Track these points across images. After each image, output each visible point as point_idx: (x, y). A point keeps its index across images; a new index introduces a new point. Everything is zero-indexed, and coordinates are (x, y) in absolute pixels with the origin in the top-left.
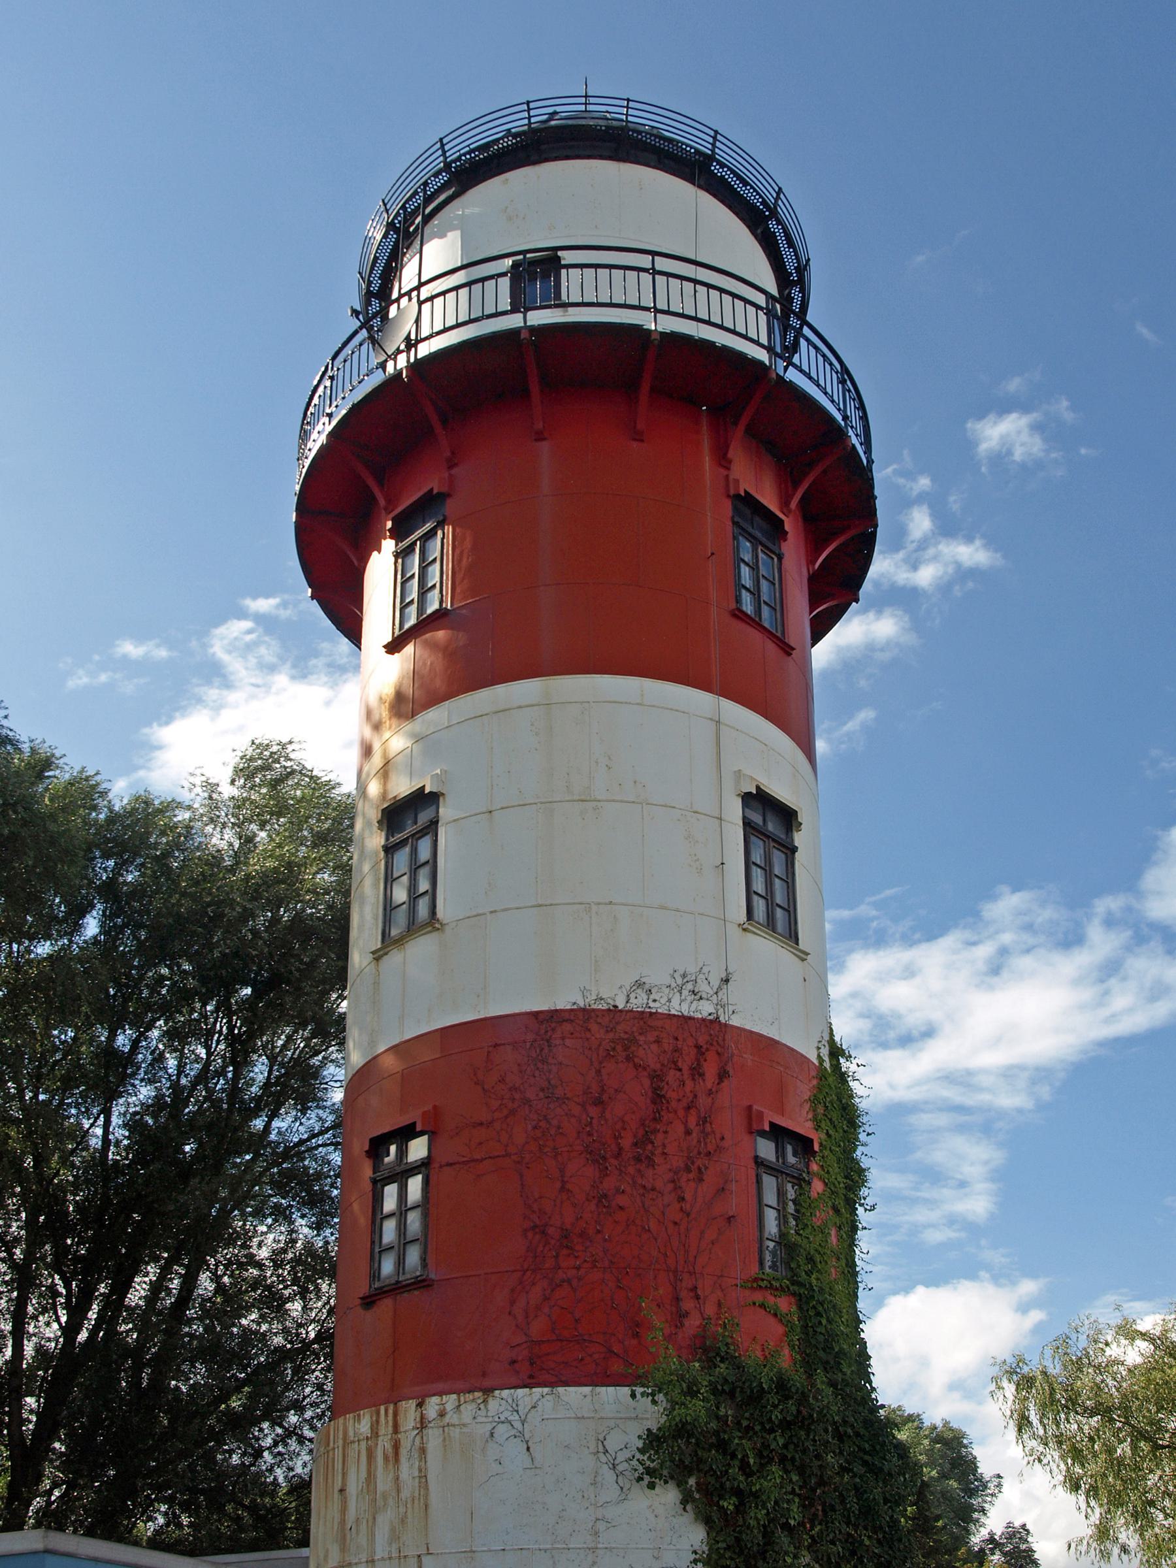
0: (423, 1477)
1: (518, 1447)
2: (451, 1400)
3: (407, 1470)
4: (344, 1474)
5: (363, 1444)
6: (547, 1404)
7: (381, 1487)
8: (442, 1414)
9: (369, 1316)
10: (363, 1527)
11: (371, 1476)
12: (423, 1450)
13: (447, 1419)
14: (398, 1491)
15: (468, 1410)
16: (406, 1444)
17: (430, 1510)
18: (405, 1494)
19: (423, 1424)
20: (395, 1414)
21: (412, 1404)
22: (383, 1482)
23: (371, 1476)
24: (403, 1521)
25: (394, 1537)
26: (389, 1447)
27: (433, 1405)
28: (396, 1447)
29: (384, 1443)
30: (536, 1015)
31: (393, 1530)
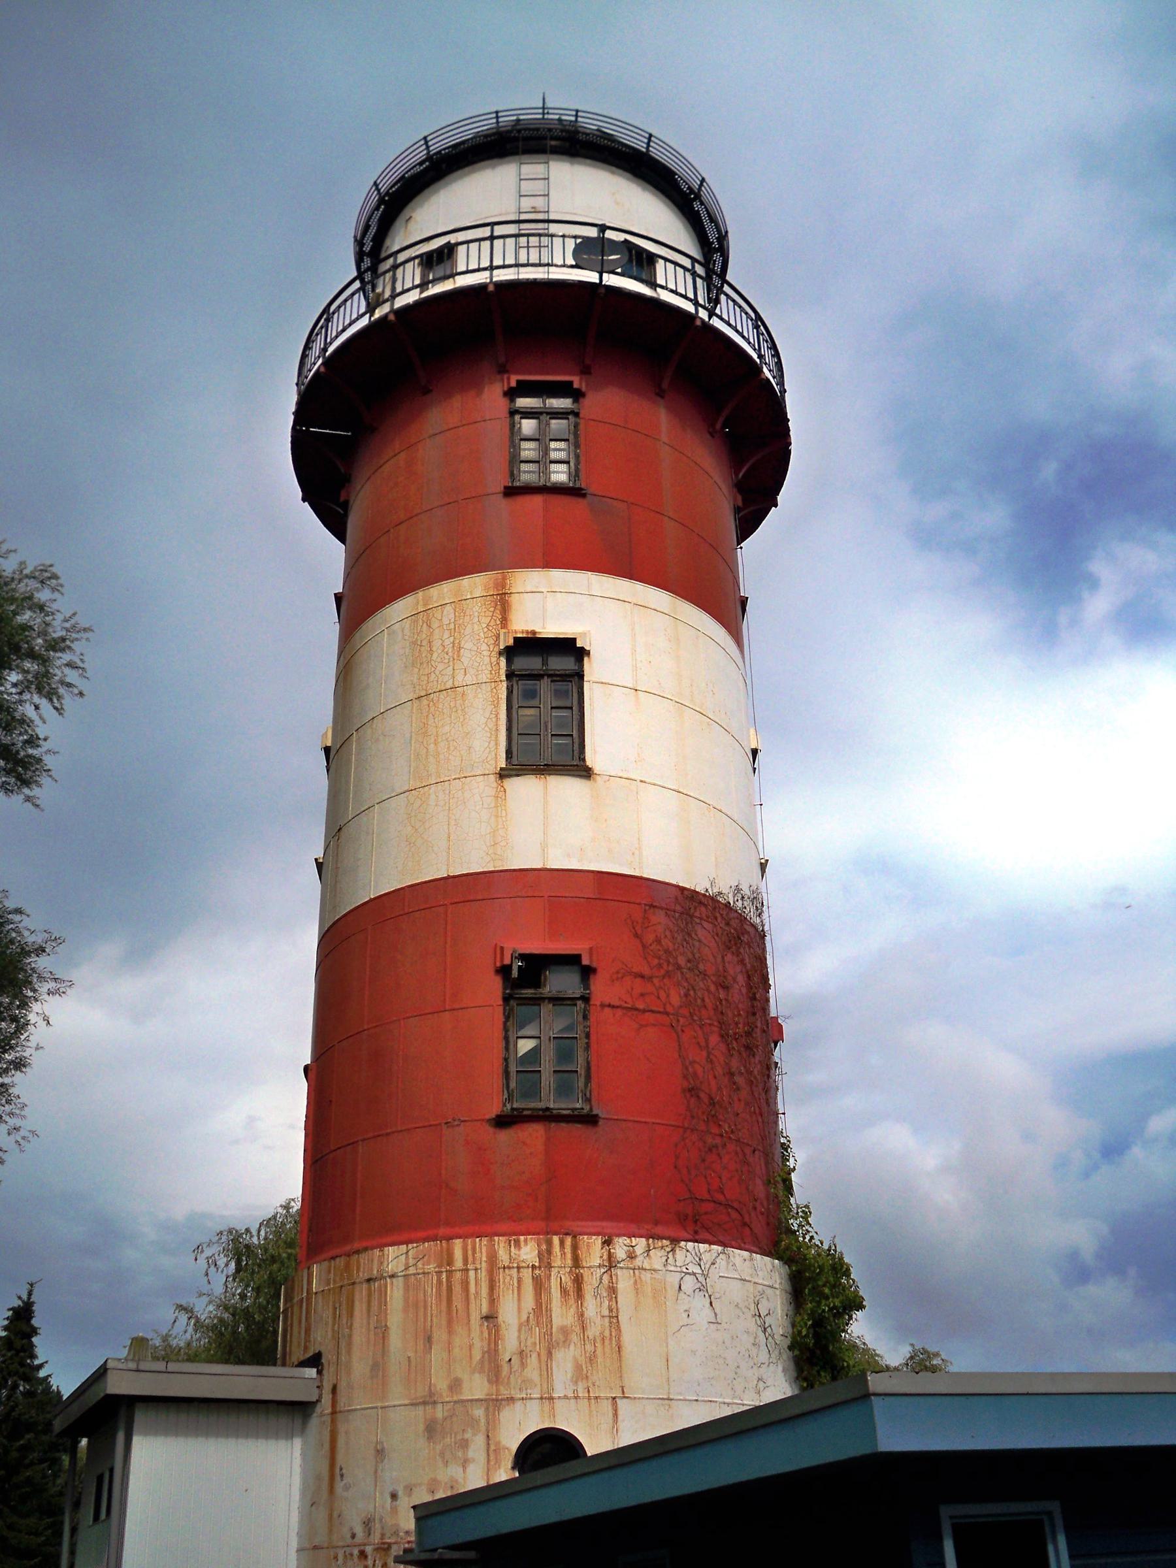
0: (614, 1317)
1: (700, 1302)
2: (640, 1244)
3: (591, 1307)
4: (493, 1301)
5: (527, 1275)
6: (722, 1261)
7: (557, 1321)
8: (631, 1256)
9: (505, 1137)
10: (533, 1361)
11: (541, 1309)
12: (613, 1290)
13: (638, 1262)
14: (584, 1329)
15: (657, 1258)
16: (592, 1279)
17: (623, 1353)
18: (593, 1331)
19: (611, 1263)
20: (575, 1247)
21: (597, 1241)
22: (561, 1315)
23: (541, 1309)
24: (592, 1359)
25: (580, 1374)
26: (567, 1280)
27: (620, 1247)
28: (578, 1281)
29: (560, 1275)
30: (683, 889)
31: (578, 1367)
